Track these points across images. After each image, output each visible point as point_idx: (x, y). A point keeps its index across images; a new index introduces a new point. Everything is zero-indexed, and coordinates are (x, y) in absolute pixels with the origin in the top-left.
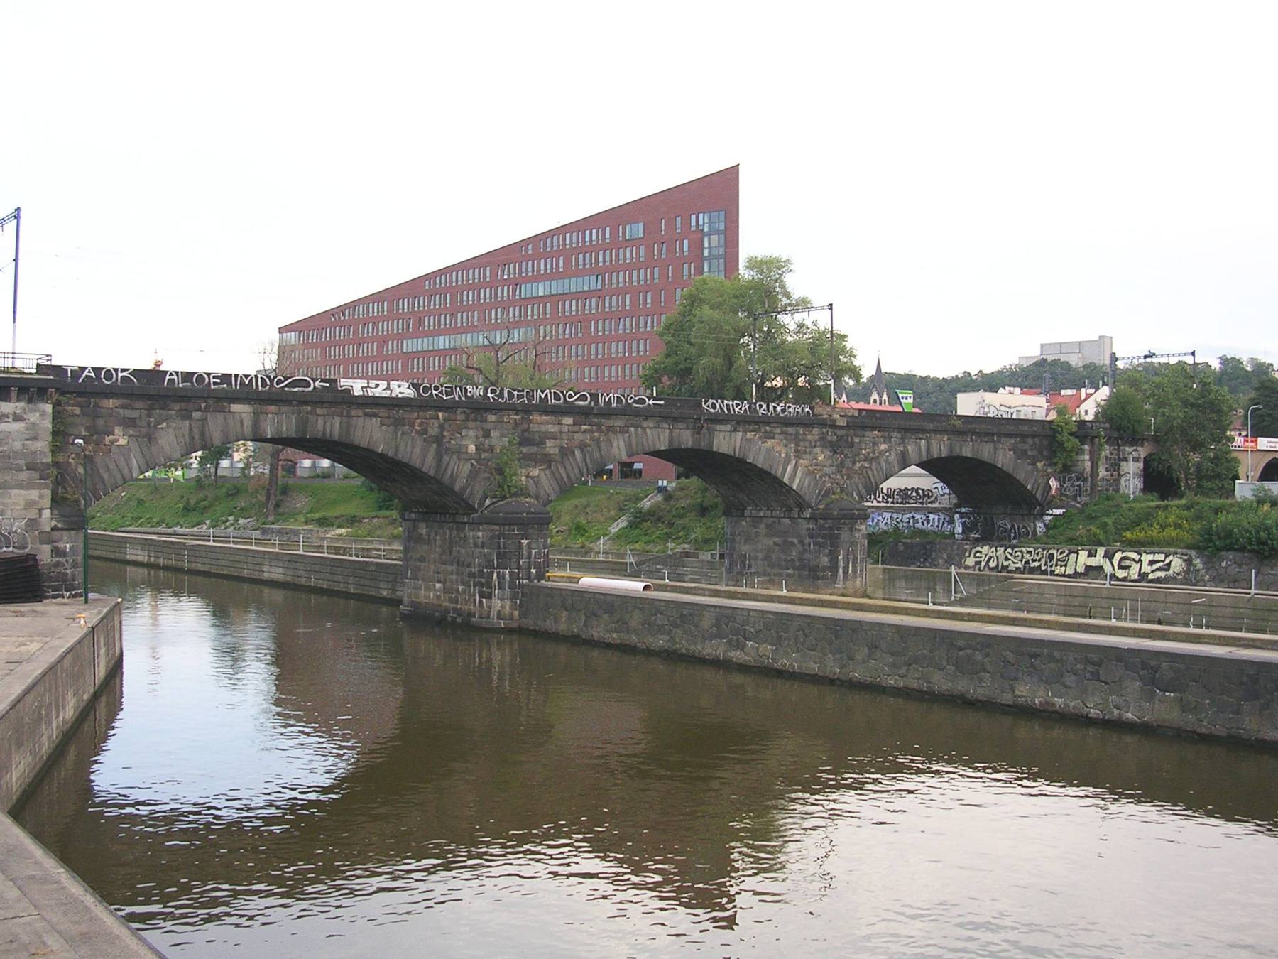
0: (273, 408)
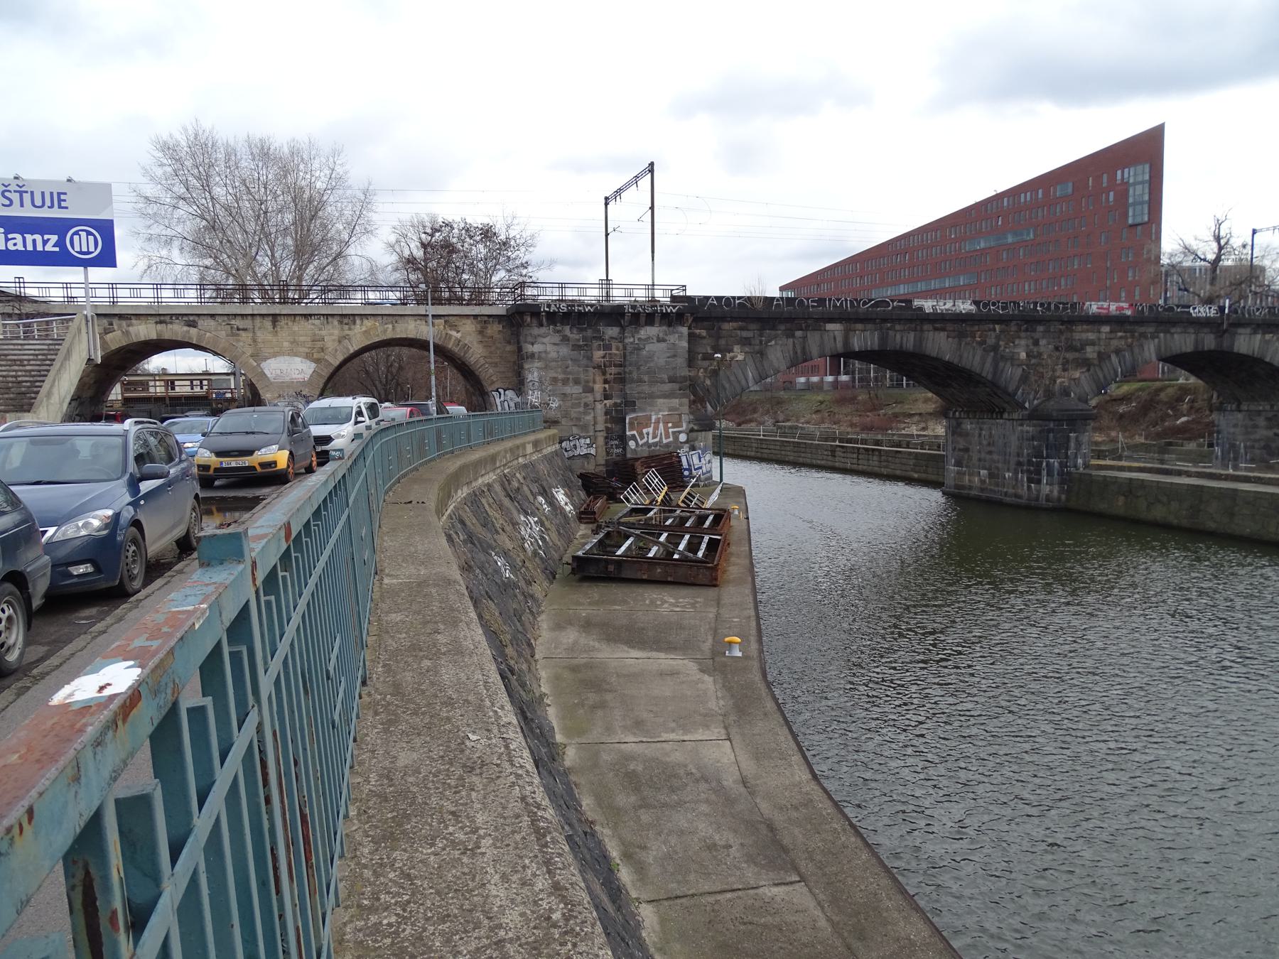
0: (859, 326)
